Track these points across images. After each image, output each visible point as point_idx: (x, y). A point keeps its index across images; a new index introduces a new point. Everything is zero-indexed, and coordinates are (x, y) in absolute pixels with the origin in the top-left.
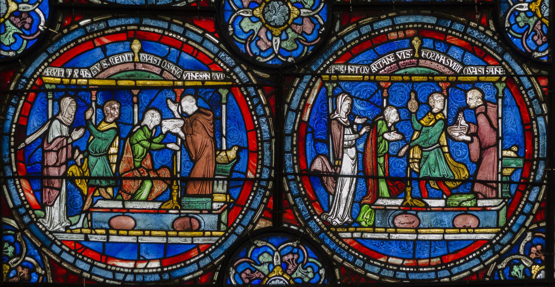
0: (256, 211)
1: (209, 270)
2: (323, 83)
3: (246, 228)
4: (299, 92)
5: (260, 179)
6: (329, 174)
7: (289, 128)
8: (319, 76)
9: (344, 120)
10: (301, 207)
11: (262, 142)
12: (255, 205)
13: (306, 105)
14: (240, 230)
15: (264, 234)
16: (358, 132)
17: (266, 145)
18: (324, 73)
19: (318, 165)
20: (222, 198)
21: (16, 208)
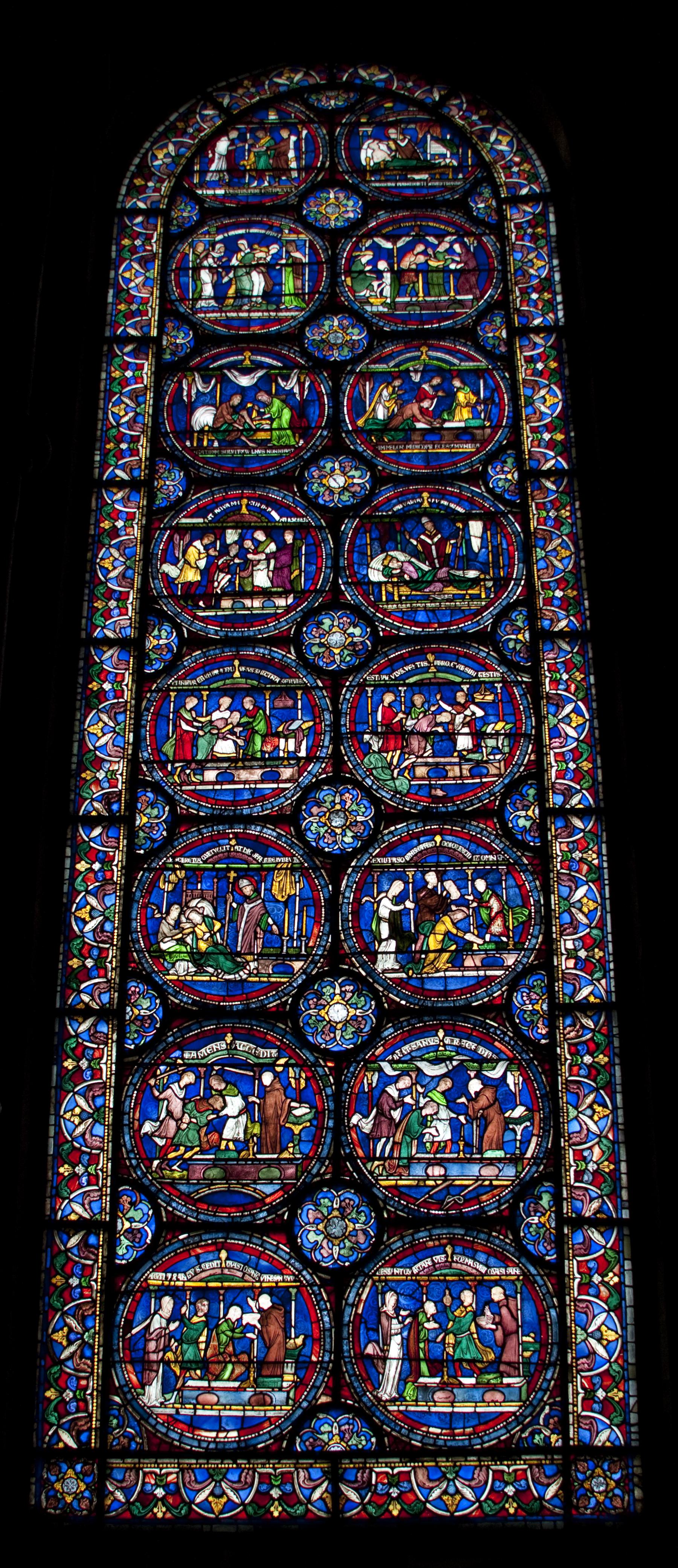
0: (319, 1388)
1: (279, 1439)
2: (374, 1282)
3: (310, 1402)
4: (354, 1290)
5: (322, 1362)
6: (378, 1357)
7: (347, 1319)
8: (370, 1277)
9: (391, 1312)
10: (356, 1384)
11: (324, 1330)
12: (318, 1384)
13: (360, 1300)
14: (305, 1404)
15: (325, 1408)
16: (403, 1322)
17: (327, 1333)
18: (374, 1274)
19: (370, 1350)
20: (291, 1378)
21: (121, 1387)
